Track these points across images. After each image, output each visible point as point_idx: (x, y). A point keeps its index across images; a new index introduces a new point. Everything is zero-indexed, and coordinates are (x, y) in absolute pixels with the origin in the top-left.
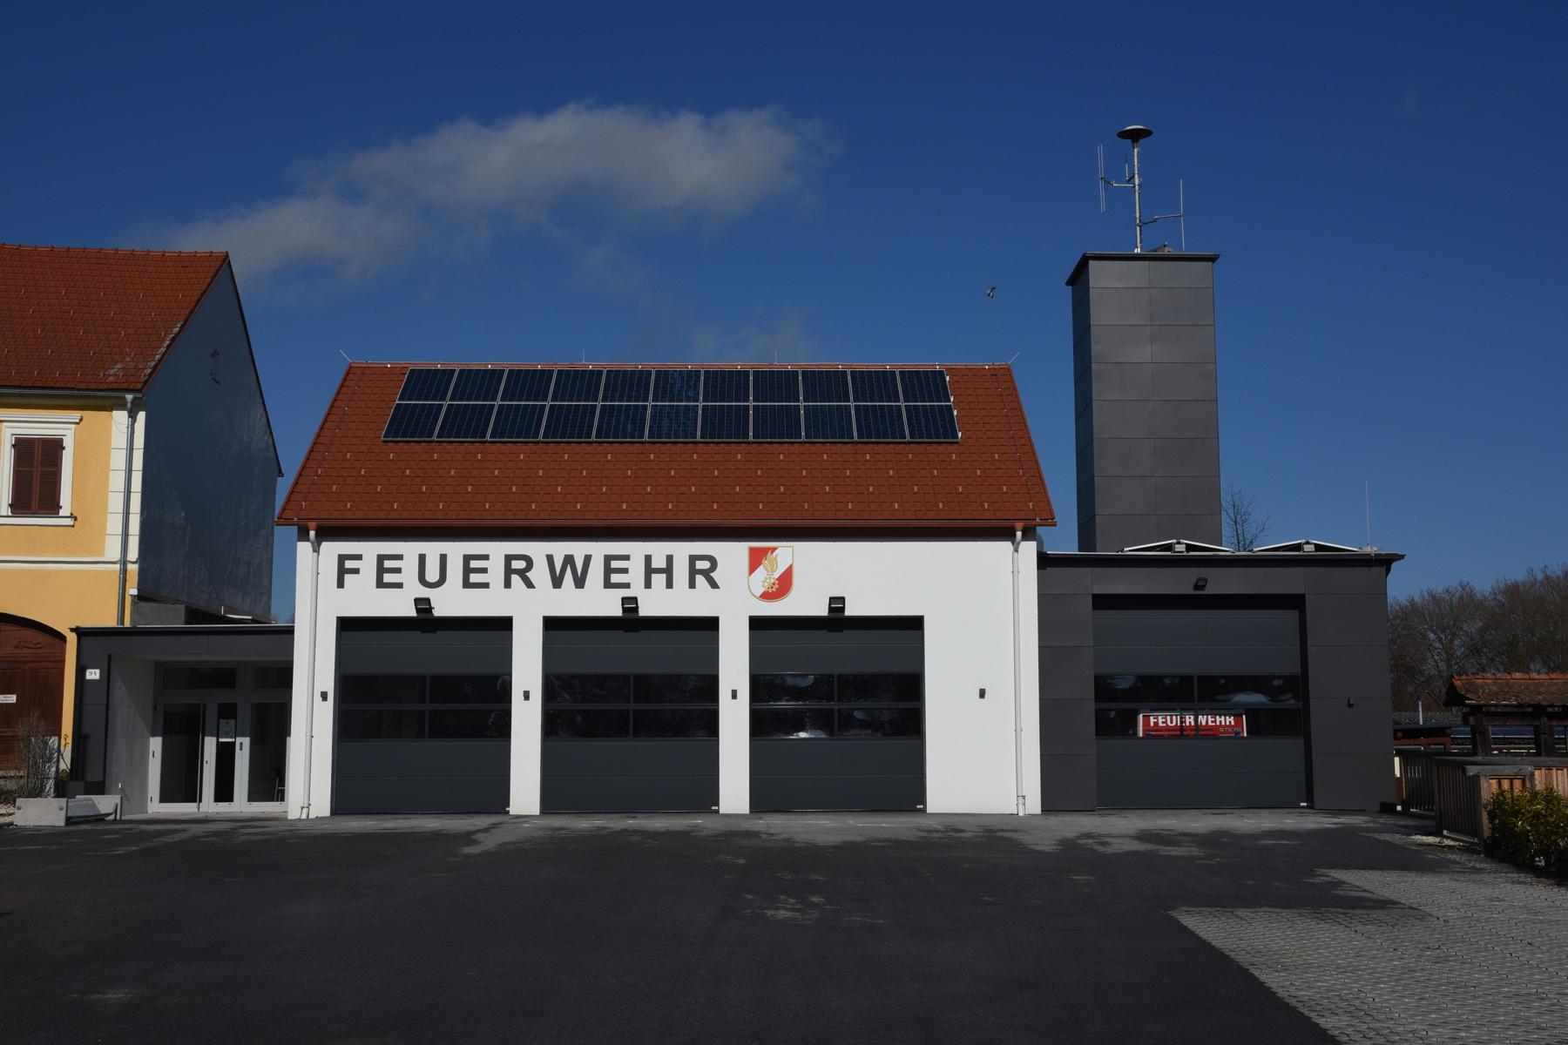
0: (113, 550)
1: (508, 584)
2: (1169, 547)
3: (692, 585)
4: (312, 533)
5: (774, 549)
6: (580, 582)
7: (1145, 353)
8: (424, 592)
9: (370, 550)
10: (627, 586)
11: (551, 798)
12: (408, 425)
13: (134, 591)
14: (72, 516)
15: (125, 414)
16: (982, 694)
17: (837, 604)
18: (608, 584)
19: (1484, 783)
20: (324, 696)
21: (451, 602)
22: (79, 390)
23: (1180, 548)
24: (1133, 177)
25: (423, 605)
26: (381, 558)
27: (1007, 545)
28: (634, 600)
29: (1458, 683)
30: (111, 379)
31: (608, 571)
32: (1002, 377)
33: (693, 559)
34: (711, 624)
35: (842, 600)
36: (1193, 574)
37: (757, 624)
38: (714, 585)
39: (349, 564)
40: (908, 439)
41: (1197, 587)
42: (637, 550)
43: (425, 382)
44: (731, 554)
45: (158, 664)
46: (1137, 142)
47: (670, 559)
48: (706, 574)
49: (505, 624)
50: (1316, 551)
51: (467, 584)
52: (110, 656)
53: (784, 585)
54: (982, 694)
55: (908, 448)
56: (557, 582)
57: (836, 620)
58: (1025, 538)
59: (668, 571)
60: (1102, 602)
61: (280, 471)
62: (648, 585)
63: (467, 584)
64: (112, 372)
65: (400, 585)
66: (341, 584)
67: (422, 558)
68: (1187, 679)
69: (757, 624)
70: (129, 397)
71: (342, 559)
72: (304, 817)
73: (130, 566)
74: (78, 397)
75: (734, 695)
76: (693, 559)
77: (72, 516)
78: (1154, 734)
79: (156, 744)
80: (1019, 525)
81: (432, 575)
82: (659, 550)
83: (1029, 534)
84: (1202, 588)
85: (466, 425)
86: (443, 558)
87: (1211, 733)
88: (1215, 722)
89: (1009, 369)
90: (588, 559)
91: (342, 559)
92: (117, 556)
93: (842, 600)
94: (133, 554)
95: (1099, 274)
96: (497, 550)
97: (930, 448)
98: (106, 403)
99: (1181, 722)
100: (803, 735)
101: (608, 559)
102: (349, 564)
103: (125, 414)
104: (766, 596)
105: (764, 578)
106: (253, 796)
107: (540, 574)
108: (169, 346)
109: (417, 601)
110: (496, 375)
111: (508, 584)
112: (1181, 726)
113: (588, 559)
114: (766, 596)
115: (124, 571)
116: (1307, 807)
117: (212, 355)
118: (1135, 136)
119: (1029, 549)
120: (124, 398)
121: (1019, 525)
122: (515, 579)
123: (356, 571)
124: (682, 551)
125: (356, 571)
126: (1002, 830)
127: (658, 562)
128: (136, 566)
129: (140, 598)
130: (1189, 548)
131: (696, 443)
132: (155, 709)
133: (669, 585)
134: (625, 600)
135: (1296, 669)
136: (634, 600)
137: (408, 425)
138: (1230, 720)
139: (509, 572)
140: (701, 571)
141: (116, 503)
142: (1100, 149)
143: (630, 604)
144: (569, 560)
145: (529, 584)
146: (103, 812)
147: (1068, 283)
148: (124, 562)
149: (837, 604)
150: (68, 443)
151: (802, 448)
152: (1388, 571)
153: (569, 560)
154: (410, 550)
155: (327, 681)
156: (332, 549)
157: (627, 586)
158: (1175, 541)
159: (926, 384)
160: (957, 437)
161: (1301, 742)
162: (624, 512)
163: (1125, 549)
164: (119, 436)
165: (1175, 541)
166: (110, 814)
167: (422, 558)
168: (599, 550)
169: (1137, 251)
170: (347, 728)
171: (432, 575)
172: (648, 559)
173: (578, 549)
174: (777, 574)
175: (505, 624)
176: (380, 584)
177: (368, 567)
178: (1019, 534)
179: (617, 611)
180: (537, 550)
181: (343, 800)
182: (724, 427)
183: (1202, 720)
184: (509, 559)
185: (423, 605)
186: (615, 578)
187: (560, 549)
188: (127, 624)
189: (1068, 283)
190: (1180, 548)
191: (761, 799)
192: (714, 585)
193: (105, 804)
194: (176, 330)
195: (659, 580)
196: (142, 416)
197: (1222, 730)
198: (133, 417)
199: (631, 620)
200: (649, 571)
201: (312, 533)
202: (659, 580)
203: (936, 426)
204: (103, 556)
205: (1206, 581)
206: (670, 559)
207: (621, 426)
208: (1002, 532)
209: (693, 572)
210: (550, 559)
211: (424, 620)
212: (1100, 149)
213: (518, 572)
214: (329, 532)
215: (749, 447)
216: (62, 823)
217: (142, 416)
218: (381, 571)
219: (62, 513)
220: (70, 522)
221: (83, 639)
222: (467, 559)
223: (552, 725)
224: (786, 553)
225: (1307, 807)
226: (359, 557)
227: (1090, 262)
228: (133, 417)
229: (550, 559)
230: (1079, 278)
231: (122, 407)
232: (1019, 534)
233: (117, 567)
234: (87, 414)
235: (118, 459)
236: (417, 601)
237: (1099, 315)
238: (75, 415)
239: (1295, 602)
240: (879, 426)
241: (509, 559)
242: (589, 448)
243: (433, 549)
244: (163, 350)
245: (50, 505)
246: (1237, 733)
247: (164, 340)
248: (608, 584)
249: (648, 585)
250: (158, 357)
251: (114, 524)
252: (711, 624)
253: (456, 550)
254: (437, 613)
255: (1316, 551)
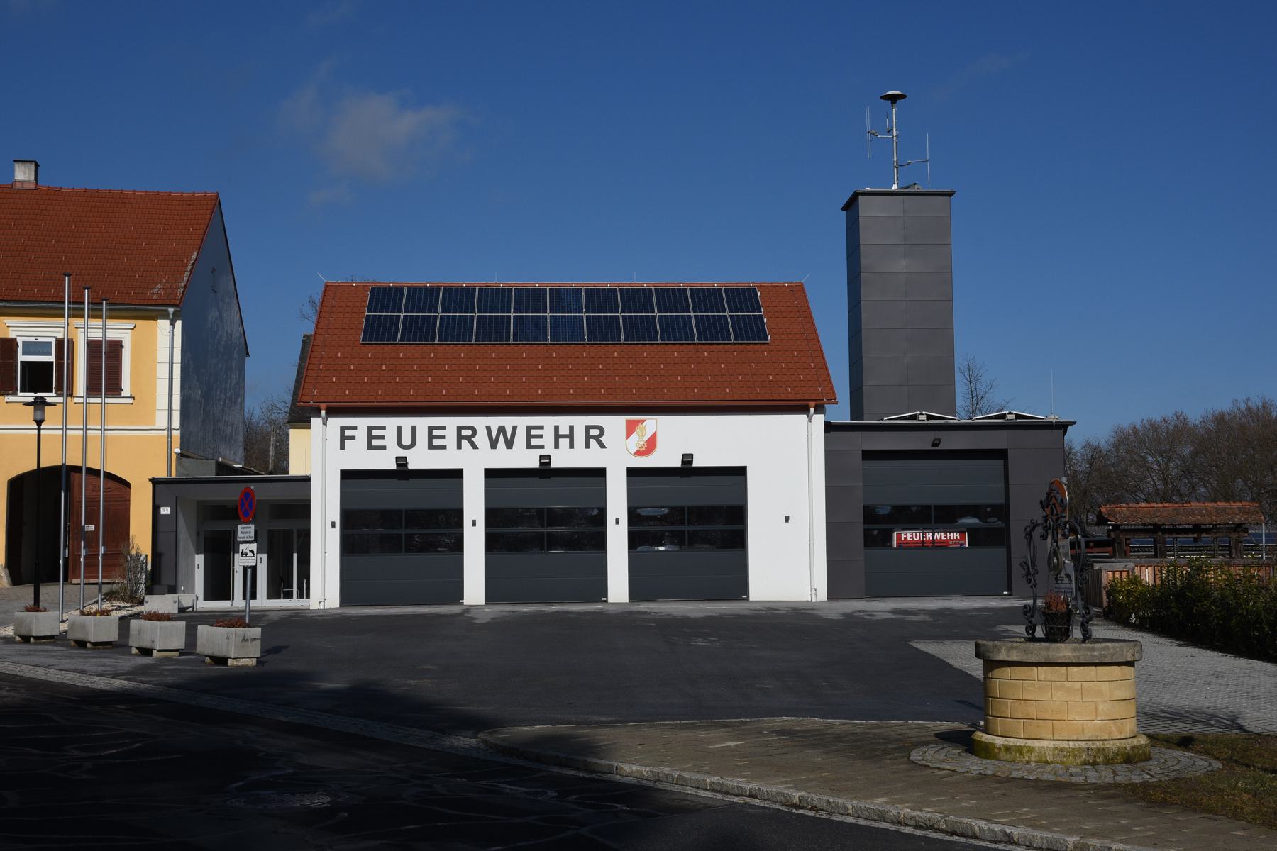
0: (162, 421)
1: (459, 447)
2: (915, 417)
3: (587, 446)
4: (323, 412)
5: (644, 421)
6: (509, 445)
7: (900, 265)
8: (402, 453)
9: (363, 423)
10: (542, 447)
11: (492, 595)
12: (378, 331)
13: (178, 451)
14: (131, 397)
15: (168, 322)
16: (787, 519)
17: (688, 459)
18: (529, 446)
19: (1104, 574)
20: (333, 525)
21: (420, 459)
22: (134, 305)
23: (923, 417)
24: (892, 130)
25: (401, 462)
26: (370, 429)
27: (804, 417)
28: (548, 457)
29: (1103, 510)
30: (155, 297)
31: (529, 437)
32: (797, 292)
33: (588, 428)
34: (600, 473)
35: (691, 456)
36: (930, 436)
37: (632, 472)
38: (602, 446)
39: (348, 433)
40: (733, 341)
41: (934, 445)
42: (549, 422)
43: (384, 297)
44: (614, 425)
45: (199, 502)
46: (895, 103)
47: (571, 428)
48: (597, 438)
49: (457, 474)
50: (1016, 419)
51: (431, 446)
52: (176, 498)
53: (651, 445)
54: (787, 519)
55: (732, 346)
56: (494, 445)
57: (687, 469)
58: (816, 412)
59: (571, 436)
60: (868, 455)
61: (248, 353)
62: (557, 446)
63: (431, 446)
64: (155, 291)
65: (384, 448)
66: (342, 447)
67: (399, 428)
68: (927, 508)
69: (632, 472)
70: (171, 310)
71: (343, 429)
72: (322, 608)
73: (174, 433)
74: (135, 310)
75: (617, 521)
76: (588, 428)
77: (131, 397)
78: (904, 546)
79: (200, 559)
80: (812, 404)
81: (407, 440)
82: (564, 422)
83: (819, 409)
84: (937, 445)
85: (419, 331)
86: (414, 428)
87: (943, 545)
88: (946, 537)
89: (802, 286)
90: (515, 428)
91: (343, 429)
92: (165, 425)
93: (691, 456)
94: (176, 423)
95: (867, 207)
96: (451, 423)
97: (749, 347)
98: (154, 314)
99: (923, 537)
100: (661, 548)
101: (529, 428)
102: (348, 433)
103: (168, 322)
104: (639, 453)
105: (637, 441)
106: (269, 597)
107: (482, 439)
108: (191, 270)
109: (398, 459)
110: (433, 292)
111: (459, 447)
112: (923, 540)
113: (515, 428)
114: (639, 453)
115: (170, 436)
116: (1008, 595)
117: (212, 272)
118: (894, 99)
119: (819, 420)
120: (167, 310)
121: (812, 404)
122: (464, 442)
123: (353, 438)
124: (580, 422)
125: (353, 438)
126: (804, 609)
127: (564, 430)
128: (179, 432)
129: (182, 455)
130: (929, 417)
131: (584, 344)
132: (198, 534)
133: (572, 446)
134: (542, 457)
135: (1001, 501)
136: (548, 457)
137: (378, 331)
138: (957, 536)
139: (460, 438)
140: (595, 437)
141: (163, 387)
142: (867, 110)
143: (545, 460)
144: (502, 429)
145: (474, 446)
146: (185, 606)
147: (843, 209)
148: (170, 429)
149: (688, 459)
150: (127, 344)
151: (659, 348)
152: (1065, 433)
153: (502, 429)
154: (391, 423)
155: (335, 514)
156: (336, 423)
157: (542, 447)
158: (919, 412)
159: (744, 298)
160: (768, 340)
161: (1003, 550)
162: (539, 396)
163: (885, 419)
164: (163, 339)
165: (919, 412)
166: (189, 608)
167: (399, 428)
168: (522, 422)
169: (894, 188)
170: (349, 546)
171: (407, 440)
172: (557, 428)
173: (508, 422)
174: (646, 438)
175: (457, 474)
176: (370, 447)
177: (361, 435)
178: (812, 410)
179: (536, 465)
180: (479, 422)
181: (347, 596)
182: (603, 332)
183: (937, 535)
184: (460, 429)
185: (401, 462)
186: (534, 442)
187: (495, 422)
188: (174, 476)
189: (843, 209)
190: (923, 417)
191: (636, 592)
192: (602, 446)
193: (186, 601)
194: (194, 257)
195: (564, 443)
196: (179, 323)
197: (951, 542)
198: (173, 324)
199: (545, 471)
200: (558, 436)
201: (323, 412)
202: (564, 443)
203: (752, 331)
204: (154, 424)
205: (940, 440)
206: (571, 428)
207: (530, 332)
208: (802, 409)
209: (588, 437)
210: (488, 428)
211: (402, 471)
212: (867, 110)
213: (466, 438)
214: (334, 411)
215: (622, 347)
216: (176, 612)
217: (179, 323)
218: (371, 437)
219: (123, 394)
220: (130, 401)
221: (157, 486)
222: (431, 429)
223: (492, 543)
224: (651, 423)
225: (1008, 595)
226: (355, 428)
227: (860, 197)
228: (173, 324)
229: (488, 428)
230: (851, 205)
231: (165, 316)
232: (812, 410)
233: (166, 433)
234: (139, 322)
235: (163, 355)
236: (398, 459)
237: (865, 237)
238: (130, 323)
239: (1001, 454)
240: (712, 331)
241: (460, 429)
242: (509, 348)
243: (407, 422)
244: (187, 273)
245: (115, 388)
246: (961, 545)
247: (187, 266)
248: (529, 446)
249: (557, 446)
250: (185, 279)
251: (162, 402)
252: (600, 473)
253: (423, 423)
254: (411, 466)
255: (1016, 419)
